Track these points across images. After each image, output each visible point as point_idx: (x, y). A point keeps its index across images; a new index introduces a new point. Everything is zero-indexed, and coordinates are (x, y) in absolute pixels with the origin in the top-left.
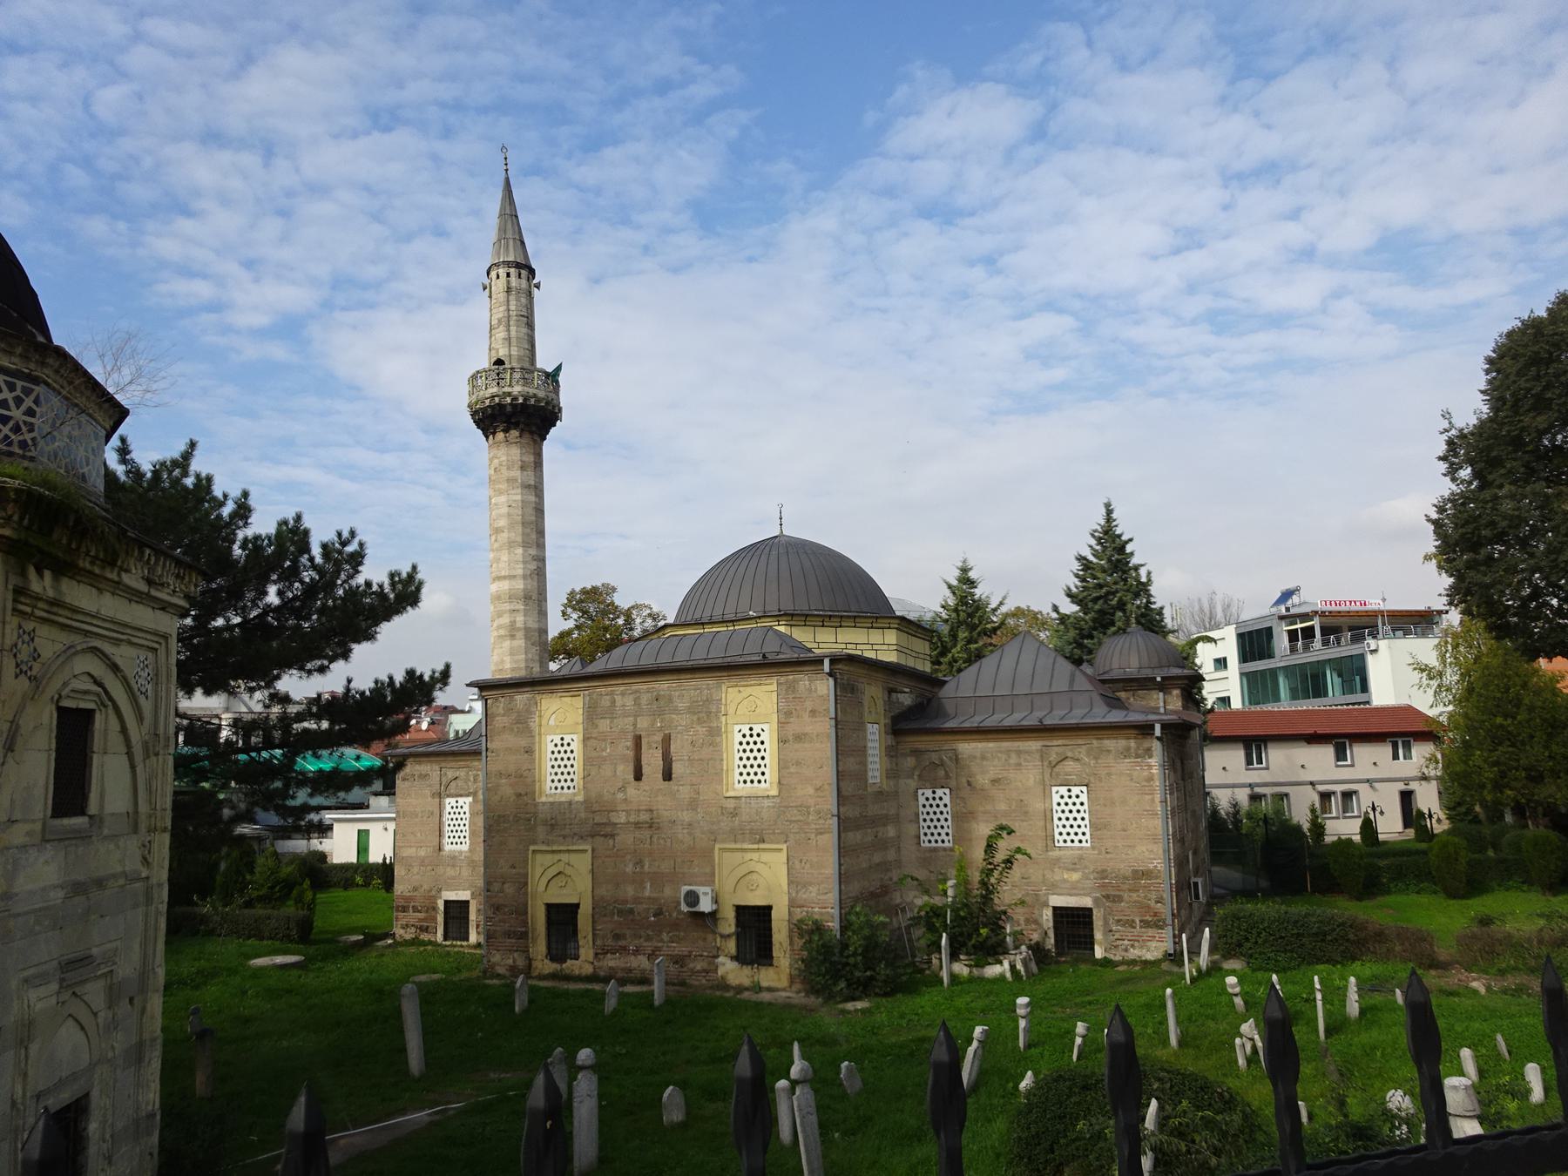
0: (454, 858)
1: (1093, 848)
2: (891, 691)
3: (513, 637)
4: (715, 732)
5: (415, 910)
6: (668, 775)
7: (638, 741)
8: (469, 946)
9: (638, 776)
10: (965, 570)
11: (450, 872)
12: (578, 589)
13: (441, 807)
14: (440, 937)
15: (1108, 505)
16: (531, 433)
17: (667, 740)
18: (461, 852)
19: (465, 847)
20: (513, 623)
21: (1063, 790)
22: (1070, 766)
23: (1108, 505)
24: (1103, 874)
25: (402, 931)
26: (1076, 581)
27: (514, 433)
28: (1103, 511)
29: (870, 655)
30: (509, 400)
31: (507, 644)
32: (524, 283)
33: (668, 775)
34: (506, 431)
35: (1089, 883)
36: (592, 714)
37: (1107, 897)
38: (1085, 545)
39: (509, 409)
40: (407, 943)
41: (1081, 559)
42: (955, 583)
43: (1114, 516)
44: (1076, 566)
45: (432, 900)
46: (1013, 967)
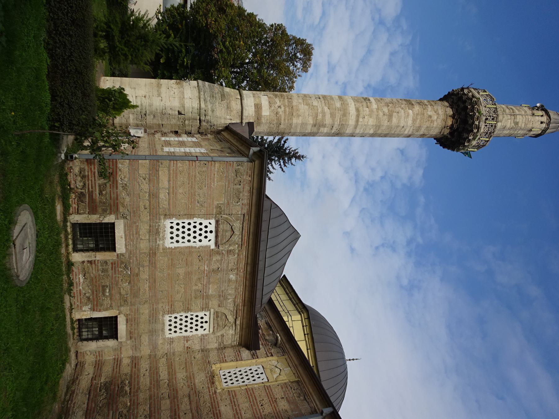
0: (158, 233)
3: (314, 125)
5: (102, 188)
8: (68, 254)
11: (144, 228)
12: (313, 51)
13: (207, 216)
14: (75, 218)
18: (164, 238)
19: (168, 243)
20: (324, 126)
25: (77, 170)
27: (447, 131)
30: (471, 138)
31: (311, 121)
34: (452, 127)
39: (465, 135)
40: (63, 177)
45: (113, 206)
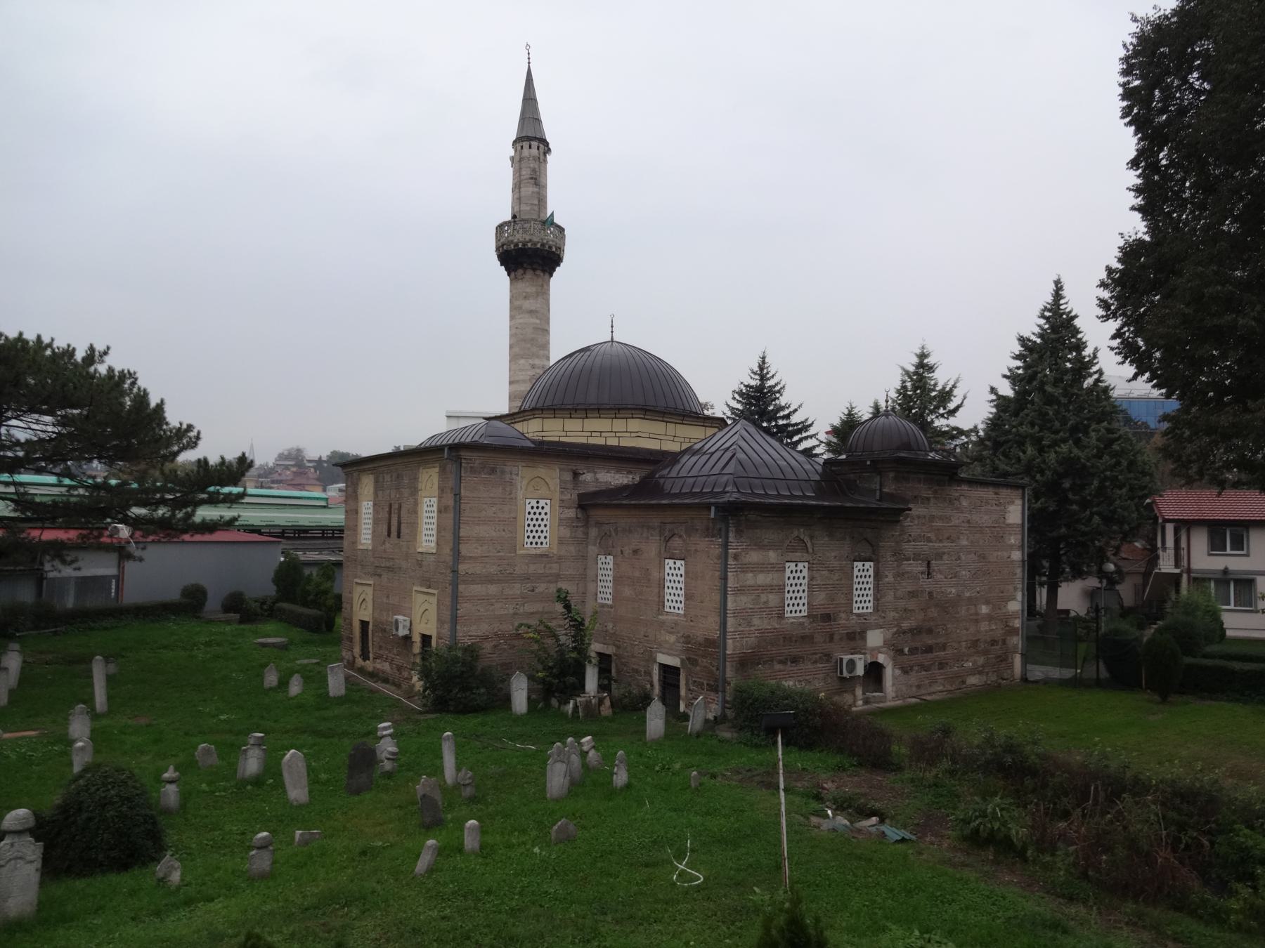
1: (685, 615)
2: (576, 475)
4: (416, 504)
6: (399, 537)
7: (391, 505)
9: (389, 535)
10: (923, 356)
15: (1058, 283)
16: (534, 270)
17: (400, 507)
21: (671, 562)
22: (676, 542)
23: (1058, 283)
24: (687, 639)
26: (1019, 363)
27: (520, 271)
28: (1053, 286)
29: (613, 442)
32: (534, 151)
33: (399, 537)
35: (679, 646)
36: (378, 487)
37: (689, 659)
38: (1031, 326)
41: (1023, 341)
42: (912, 369)
43: (1064, 293)
44: (1018, 349)
46: (576, 707)
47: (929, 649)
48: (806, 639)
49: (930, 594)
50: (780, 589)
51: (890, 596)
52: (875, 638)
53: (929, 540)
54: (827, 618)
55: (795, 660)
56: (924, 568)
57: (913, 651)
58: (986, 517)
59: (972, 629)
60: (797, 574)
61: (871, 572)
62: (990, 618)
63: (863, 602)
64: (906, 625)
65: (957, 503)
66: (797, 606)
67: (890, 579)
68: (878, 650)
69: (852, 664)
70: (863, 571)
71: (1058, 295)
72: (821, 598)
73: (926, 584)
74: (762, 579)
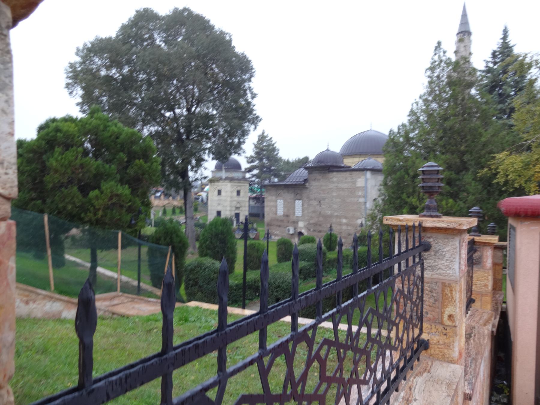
47: (320, 232)
48: (282, 221)
49: (320, 212)
50: (276, 207)
51: (306, 212)
52: (301, 224)
53: (320, 194)
54: (287, 216)
55: (280, 226)
56: (318, 203)
57: (314, 231)
58: (346, 185)
59: (339, 227)
60: (280, 203)
61: (301, 204)
62: (347, 225)
63: (298, 212)
64: (311, 222)
65: (331, 180)
66: (280, 212)
67: (306, 206)
68: (301, 228)
69: (289, 230)
70: (298, 204)
71: (505, 37)
72: (286, 210)
73: (318, 208)
74: (272, 204)
